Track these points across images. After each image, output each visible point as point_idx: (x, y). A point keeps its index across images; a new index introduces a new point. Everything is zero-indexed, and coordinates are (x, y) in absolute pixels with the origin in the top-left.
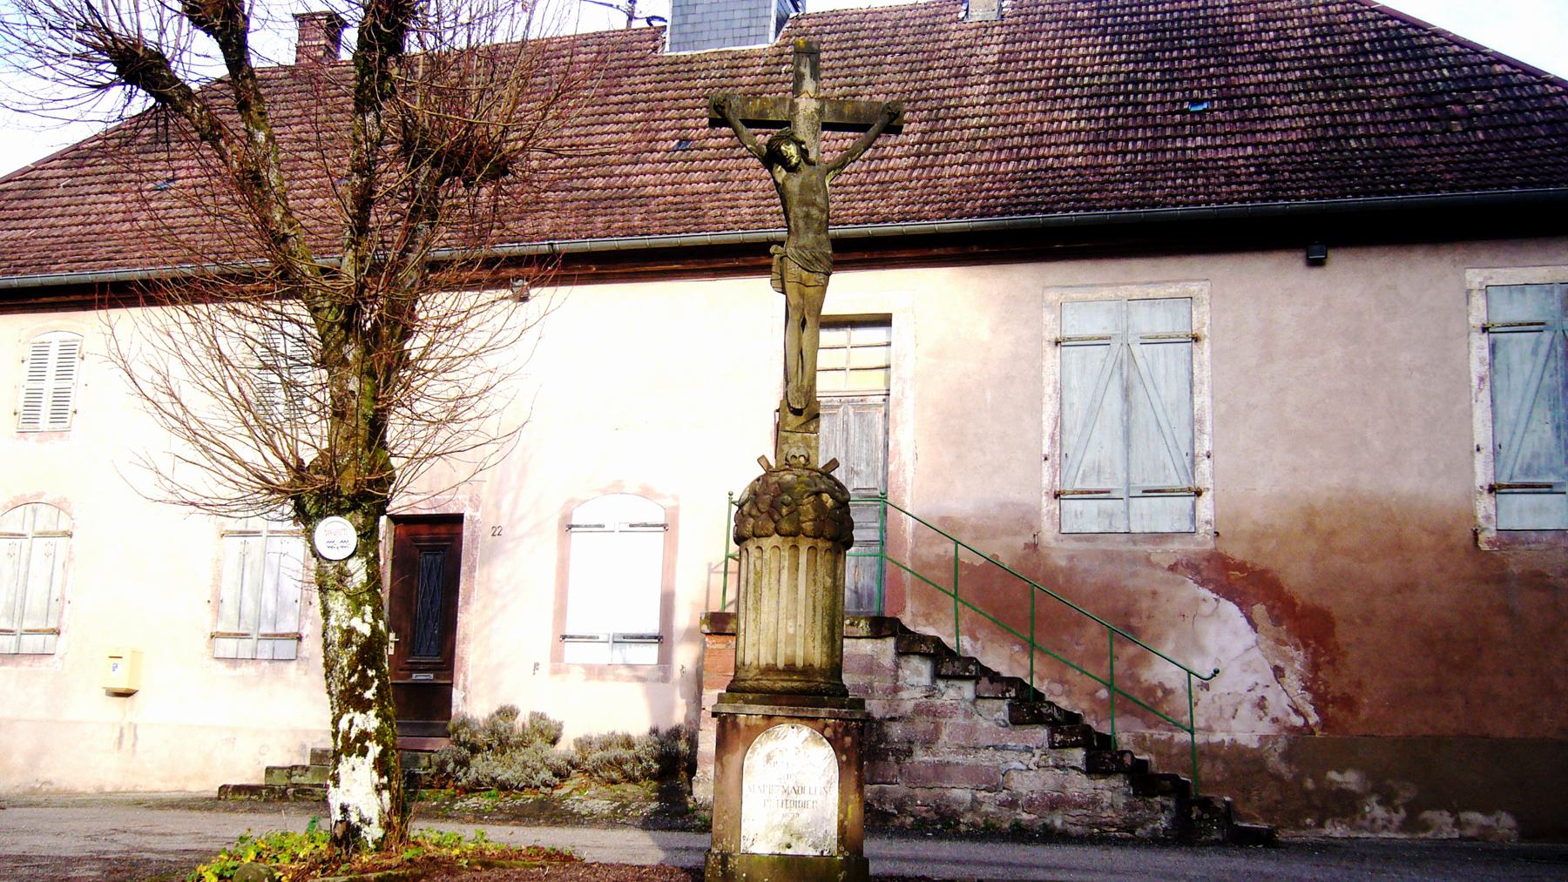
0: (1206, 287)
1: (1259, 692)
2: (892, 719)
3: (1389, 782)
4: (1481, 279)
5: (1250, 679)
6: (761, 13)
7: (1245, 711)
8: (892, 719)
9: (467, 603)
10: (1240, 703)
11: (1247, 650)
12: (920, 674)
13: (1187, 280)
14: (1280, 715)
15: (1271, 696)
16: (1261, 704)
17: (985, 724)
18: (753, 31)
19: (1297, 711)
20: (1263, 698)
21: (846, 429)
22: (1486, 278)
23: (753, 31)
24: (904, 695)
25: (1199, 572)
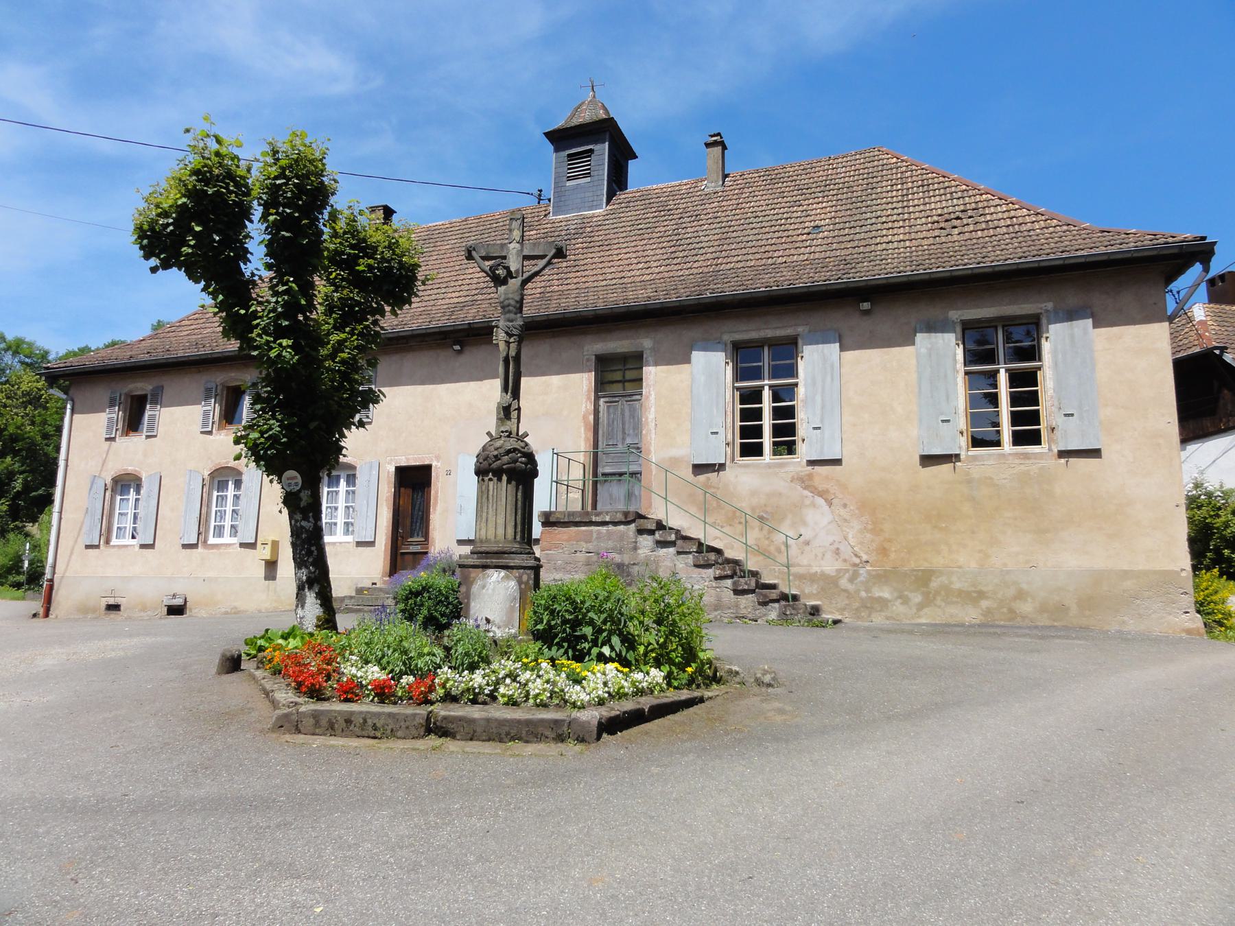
0: (806, 329)
1: (836, 546)
2: (634, 564)
3: (906, 593)
4: (957, 316)
5: (831, 539)
6: (599, 193)
7: (829, 555)
8: (634, 564)
9: (435, 510)
10: (826, 552)
11: (829, 523)
12: (648, 541)
13: (796, 325)
14: (847, 558)
15: (842, 548)
16: (837, 552)
17: (681, 566)
18: (595, 203)
19: (856, 555)
20: (838, 549)
21: (623, 415)
22: (960, 316)
23: (595, 203)
24: (640, 551)
25: (803, 482)
